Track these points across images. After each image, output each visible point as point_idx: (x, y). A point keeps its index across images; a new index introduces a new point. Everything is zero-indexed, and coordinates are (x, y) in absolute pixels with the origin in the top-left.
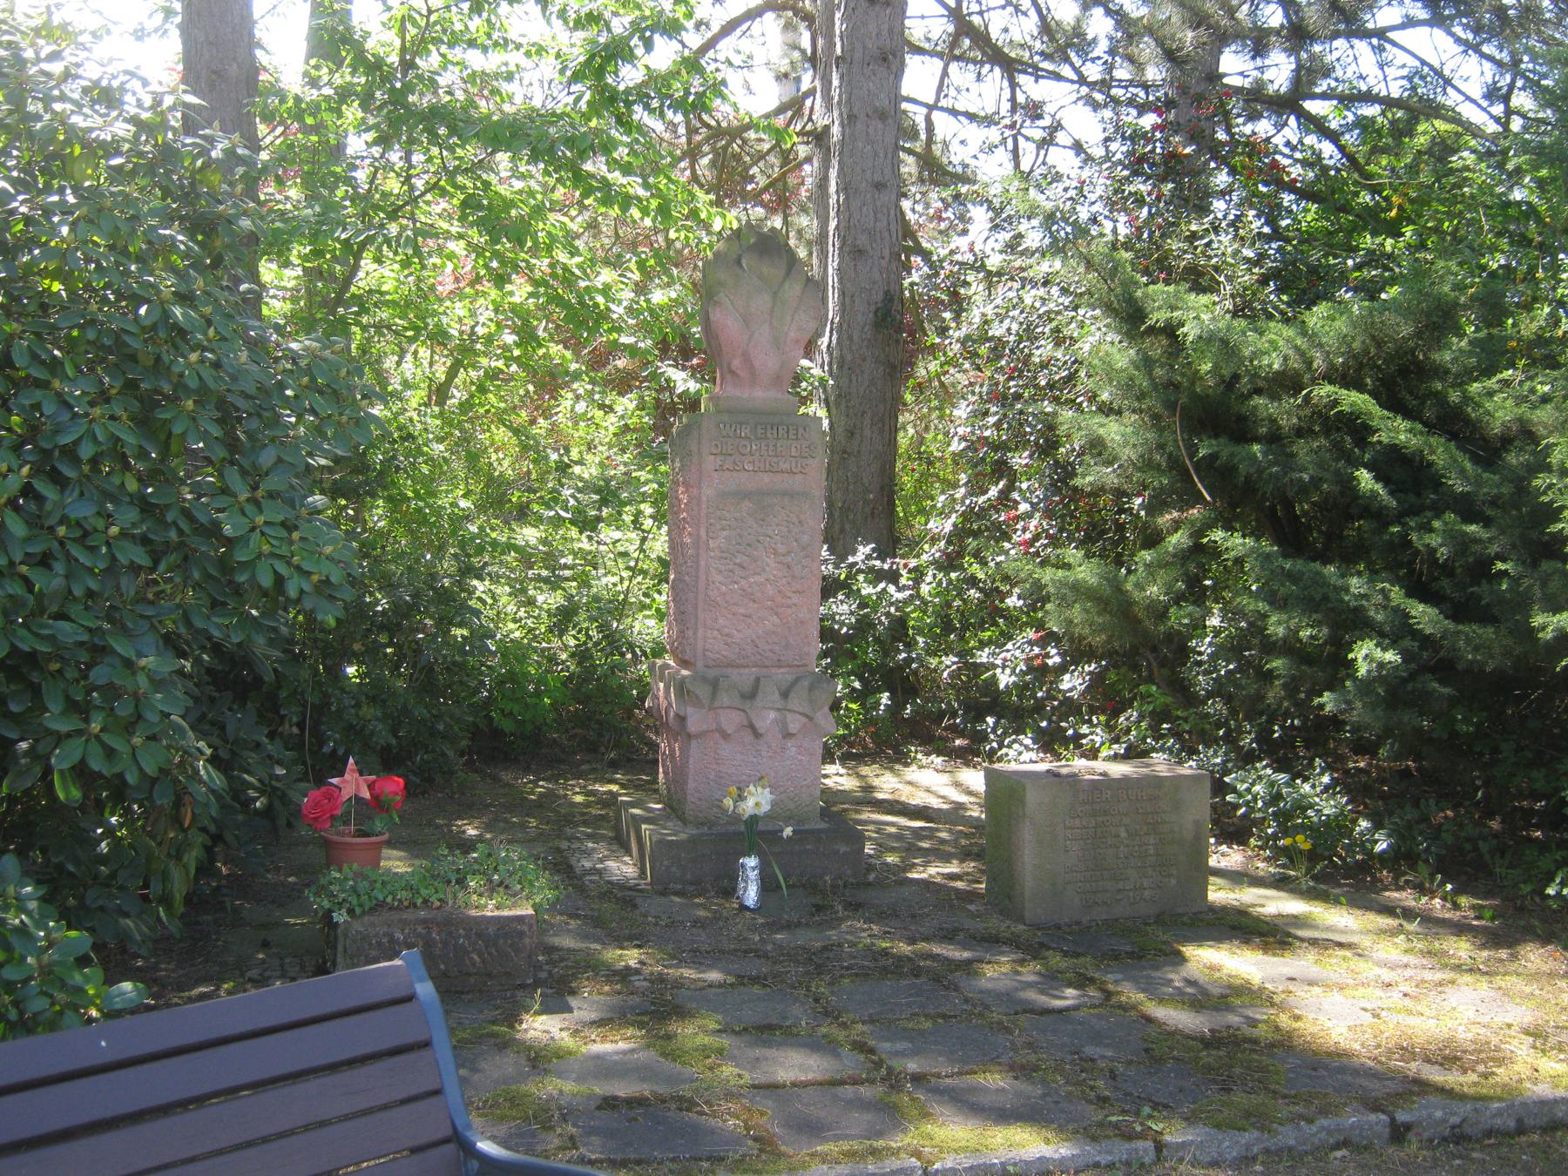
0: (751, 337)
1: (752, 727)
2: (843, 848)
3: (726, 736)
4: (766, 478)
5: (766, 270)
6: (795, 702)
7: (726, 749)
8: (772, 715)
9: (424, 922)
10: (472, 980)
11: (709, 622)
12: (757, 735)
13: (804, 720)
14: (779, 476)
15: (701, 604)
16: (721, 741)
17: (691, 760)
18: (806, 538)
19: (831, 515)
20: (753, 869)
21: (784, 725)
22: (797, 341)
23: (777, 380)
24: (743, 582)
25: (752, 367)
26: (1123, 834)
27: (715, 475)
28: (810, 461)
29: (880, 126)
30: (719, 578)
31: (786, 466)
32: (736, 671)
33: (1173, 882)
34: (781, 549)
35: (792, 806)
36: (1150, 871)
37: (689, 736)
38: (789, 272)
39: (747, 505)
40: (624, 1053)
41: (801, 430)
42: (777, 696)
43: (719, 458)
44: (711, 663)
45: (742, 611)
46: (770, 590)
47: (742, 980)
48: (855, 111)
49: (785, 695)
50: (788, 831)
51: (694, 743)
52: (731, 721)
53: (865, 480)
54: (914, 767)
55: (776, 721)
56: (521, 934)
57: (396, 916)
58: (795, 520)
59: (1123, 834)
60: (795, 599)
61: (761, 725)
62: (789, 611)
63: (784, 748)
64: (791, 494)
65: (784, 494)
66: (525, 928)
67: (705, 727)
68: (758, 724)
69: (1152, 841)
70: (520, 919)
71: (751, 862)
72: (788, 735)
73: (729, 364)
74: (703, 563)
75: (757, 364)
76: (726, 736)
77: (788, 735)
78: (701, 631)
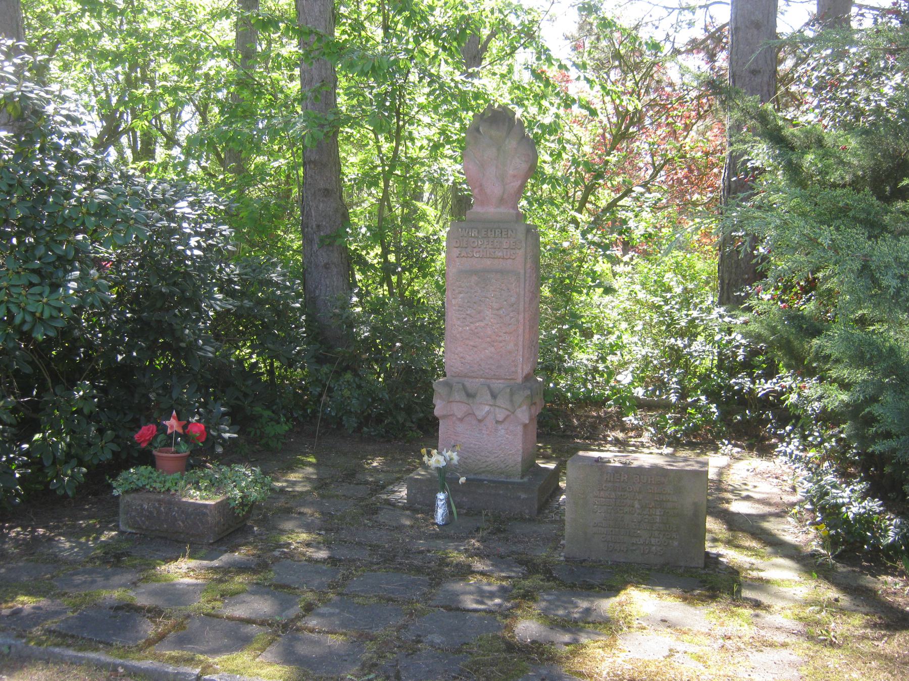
2: (523, 496)
3: (461, 420)
4: (488, 262)
5: (493, 132)
6: (501, 401)
7: (460, 427)
8: (487, 408)
9: (159, 501)
10: (182, 536)
13: (507, 413)
14: (496, 261)
18: (513, 300)
19: (722, 288)
20: (441, 500)
22: (514, 176)
23: (502, 201)
26: (637, 505)
27: (457, 260)
28: (518, 251)
29: (756, 33)
30: (459, 323)
32: (471, 380)
33: (676, 543)
35: (503, 466)
36: (656, 533)
38: (508, 133)
39: (474, 279)
40: (188, 585)
41: (510, 232)
42: (489, 397)
45: (472, 343)
46: (489, 331)
47: (333, 561)
48: (739, 25)
49: (494, 396)
50: (463, 480)
52: (459, 410)
53: (742, 266)
54: (719, 455)
56: (205, 514)
57: (151, 496)
59: (637, 505)
61: (480, 414)
63: (496, 430)
64: (502, 272)
65: (497, 272)
66: (208, 512)
67: (445, 413)
68: (477, 413)
69: (658, 513)
70: (206, 506)
71: (441, 496)
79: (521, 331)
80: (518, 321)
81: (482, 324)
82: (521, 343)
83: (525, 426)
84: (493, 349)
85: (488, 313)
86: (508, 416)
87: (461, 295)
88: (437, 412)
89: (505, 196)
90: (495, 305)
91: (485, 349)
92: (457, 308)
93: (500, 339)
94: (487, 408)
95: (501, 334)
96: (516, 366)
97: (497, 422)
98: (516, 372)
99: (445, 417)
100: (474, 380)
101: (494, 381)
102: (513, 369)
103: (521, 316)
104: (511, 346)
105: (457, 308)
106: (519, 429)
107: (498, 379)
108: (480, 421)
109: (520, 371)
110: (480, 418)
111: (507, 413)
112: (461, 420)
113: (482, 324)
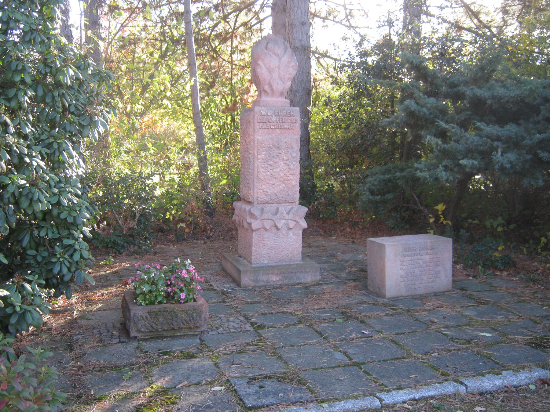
0: (272, 77)
1: (276, 226)
7: (266, 235)
11: (259, 187)
12: (278, 229)
13: (295, 223)
15: (255, 180)
16: (265, 232)
17: (253, 239)
21: (288, 225)
22: (289, 79)
27: (260, 130)
28: (295, 125)
30: (262, 170)
31: (286, 126)
34: (285, 158)
35: (291, 255)
37: (253, 230)
43: (261, 124)
44: (260, 202)
45: (271, 182)
51: (254, 233)
55: (285, 224)
58: (290, 147)
60: (291, 177)
61: (279, 225)
62: (289, 182)
63: (288, 234)
68: (278, 225)
72: (290, 229)
73: (263, 88)
74: (256, 165)
75: (274, 87)
76: (266, 230)
77: (290, 229)
78: (255, 191)
81: (278, 170)
84: (284, 185)
85: (281, 163)
87: (264, 153)
91: (279, 185)
92: (262, 161)
93: (289, 178)
105: (262, 161)
106: (300, 233)
107: (285, 203)
110: (280, 228)
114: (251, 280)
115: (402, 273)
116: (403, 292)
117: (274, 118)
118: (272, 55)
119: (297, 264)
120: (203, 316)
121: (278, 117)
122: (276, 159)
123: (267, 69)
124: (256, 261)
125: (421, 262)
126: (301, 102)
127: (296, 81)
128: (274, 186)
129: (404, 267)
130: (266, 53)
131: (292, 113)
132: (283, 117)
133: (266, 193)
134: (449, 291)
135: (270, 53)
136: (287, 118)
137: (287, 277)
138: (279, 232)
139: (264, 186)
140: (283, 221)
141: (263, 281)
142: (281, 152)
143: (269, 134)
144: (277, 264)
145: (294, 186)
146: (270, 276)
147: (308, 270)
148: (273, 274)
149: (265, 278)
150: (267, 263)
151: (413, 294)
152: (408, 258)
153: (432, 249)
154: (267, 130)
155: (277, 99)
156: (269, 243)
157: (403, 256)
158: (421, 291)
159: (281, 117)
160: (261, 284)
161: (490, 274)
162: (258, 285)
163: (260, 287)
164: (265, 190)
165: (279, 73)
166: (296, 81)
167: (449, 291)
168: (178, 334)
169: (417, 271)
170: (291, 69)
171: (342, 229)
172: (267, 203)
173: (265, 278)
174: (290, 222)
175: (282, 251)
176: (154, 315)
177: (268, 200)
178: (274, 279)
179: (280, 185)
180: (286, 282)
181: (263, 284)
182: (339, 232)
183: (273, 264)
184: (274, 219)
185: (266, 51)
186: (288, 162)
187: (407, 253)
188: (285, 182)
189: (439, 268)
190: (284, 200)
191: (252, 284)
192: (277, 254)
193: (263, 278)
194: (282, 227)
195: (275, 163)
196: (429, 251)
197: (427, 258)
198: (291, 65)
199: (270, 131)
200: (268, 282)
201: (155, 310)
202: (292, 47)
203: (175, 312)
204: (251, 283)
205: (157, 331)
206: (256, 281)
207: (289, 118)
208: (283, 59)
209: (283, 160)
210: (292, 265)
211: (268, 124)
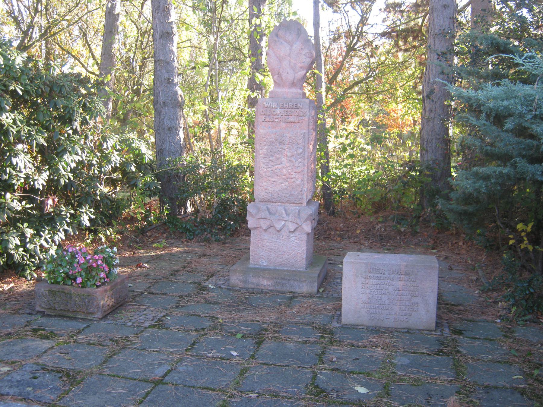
1: (274, 227)
3: (266, 230)
7: (265, 235)
18: (300, 151)
22: (301, 67)
24: (273, 168)
25: (282, 79)
28: (303, 118)
30: (264, 166)
32: (272, 204)
43: (264, 116)
45: (273, 179)
60: (297, 176)
62: (293, 180)
63: (289, 237)
67: (255, 226)
75: (284, 77)
79: (306, 171)
80: (304, 165)
81: (280, 166)
82: (305, 179)
83: (308, 234)
84: (287, 183)
85: (284, 159)
86: (297, 228)
88: (249, 225)
89: (295, 81)
90: (289, 154)
92: (263, 156)
93: (292, 176)
94: (283, 223)
95: (293, 173)
96: (302, 195)
97: (290, 232)
98: (302, 199)
99: (255, 228)
100: (274, 204)
101: (287, 204)
102: (300, 197)
103: (306, 161)
104: (299, 182)
105: (263, 156)
106: (305, 237)
108: (278, 231)
109: (305, 198)
110: (278, 229)
111: (297, 226)
112: (266, 230)
113: (280, 166)
114: (240, 280)
115: (364, 298)
116: (364, 319)
117: (278, 111)
118: (283, 42)
119: (293, 271)
120: (95, 303)
121: (283, 110)
122: (278, 154)
123: (277, 57)
124: (254, 261)
125: (391, 288)
126: (439, 95)
127: (434, 71)
128: (275, 183)
129: (368, 291)
130: (276, 41)
131: (299, 105)
132: (289, 110)
133: (267, 191)
134: (431, 331)
135: (281, 40)
136: (293, 110)
137: (279, 283)
138: (280, 233)
139: (265, 184)
140: (283, 223)
141: (253, 283)
142: (284, 147)
143: (273, 127)
144: (277, 268)
145: (298, 185)
146: (261, 279)
147: (304, 279)
148: (263, 277)
149: (255, 280)
150: (267, 266)
151: (379, 325)
152: (374, 281)
153: (407, 274)
154: (270, 123)
155: (289, 91)
156: (268, 244)
157: (366, 278)
158: (389, 323)
159: (286, 110)
160: (250, 286)
161: (530, 320)
162: (247, 286)
163: (247, 289)
164: (266, 187)
165: (290, 61)
166: (434, 71)
167: (431, 331)
168: (79, 317)
169: (385, 298)
170: (304, 57)
171: (454, 242)
172: (268, 202)
173: (255, 280)
174: (290, 224)
175: (284, 255)
176: (52, 293)
177: (269, 198)
178: (265, 283)
179: (282, 183)
180: (278, 288)
181: (253, 286)
182: (450, 245)
183: (272, 268)
184: (271, 219)
185: (276, 38)
186: (292, 159)
187: (372, 275)
188: (289, 180)
189: (416, 300)
190: (287, 199)
191: (241, 285)
192: (278, 257)
193: (254, 281)
194: (281, 229)
195: (278, 159)
196: (402, 276)
197: (400, 284)
198: (304, 53)
199: (274, 124)
200: (258, 285)
201: (55, 289)
202: (432, 33)
203: (71, 294)
204: (240, 284)
205: (55, 309)
206: (245, 282)
207: (296, 110)
208: (295, 46)
209: (287, 156)
210: (287, 271)
211: (272, 116)
